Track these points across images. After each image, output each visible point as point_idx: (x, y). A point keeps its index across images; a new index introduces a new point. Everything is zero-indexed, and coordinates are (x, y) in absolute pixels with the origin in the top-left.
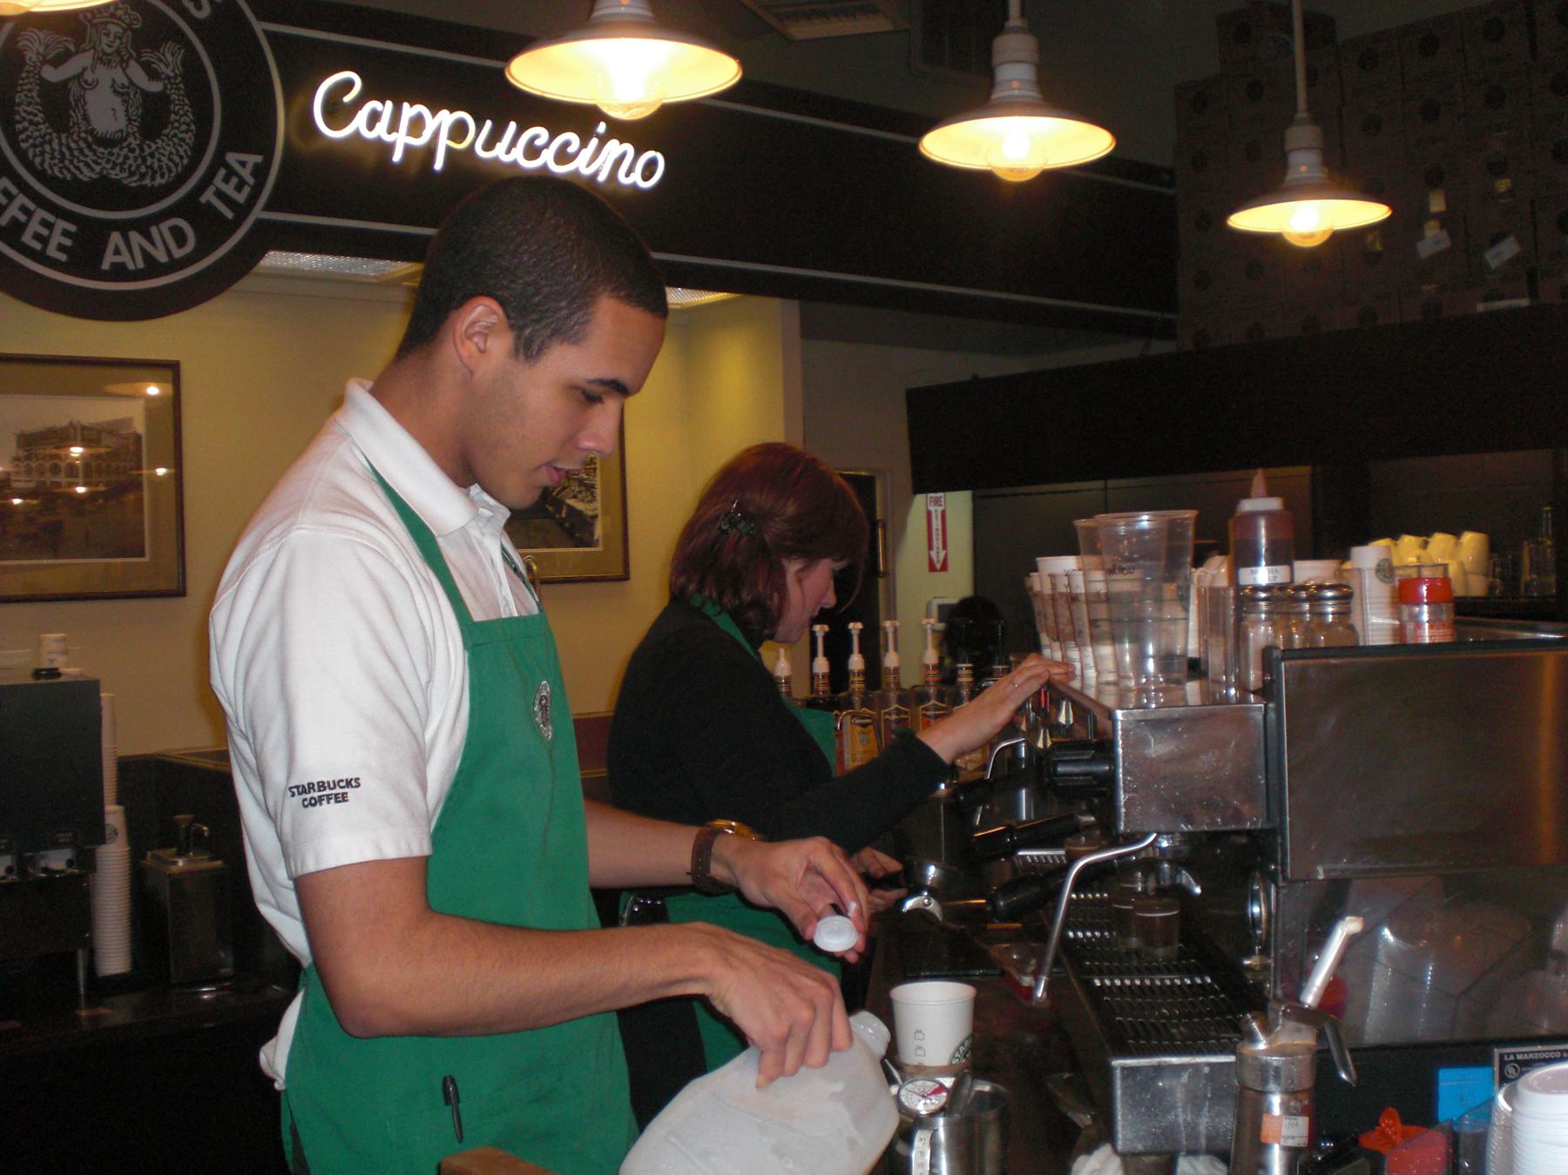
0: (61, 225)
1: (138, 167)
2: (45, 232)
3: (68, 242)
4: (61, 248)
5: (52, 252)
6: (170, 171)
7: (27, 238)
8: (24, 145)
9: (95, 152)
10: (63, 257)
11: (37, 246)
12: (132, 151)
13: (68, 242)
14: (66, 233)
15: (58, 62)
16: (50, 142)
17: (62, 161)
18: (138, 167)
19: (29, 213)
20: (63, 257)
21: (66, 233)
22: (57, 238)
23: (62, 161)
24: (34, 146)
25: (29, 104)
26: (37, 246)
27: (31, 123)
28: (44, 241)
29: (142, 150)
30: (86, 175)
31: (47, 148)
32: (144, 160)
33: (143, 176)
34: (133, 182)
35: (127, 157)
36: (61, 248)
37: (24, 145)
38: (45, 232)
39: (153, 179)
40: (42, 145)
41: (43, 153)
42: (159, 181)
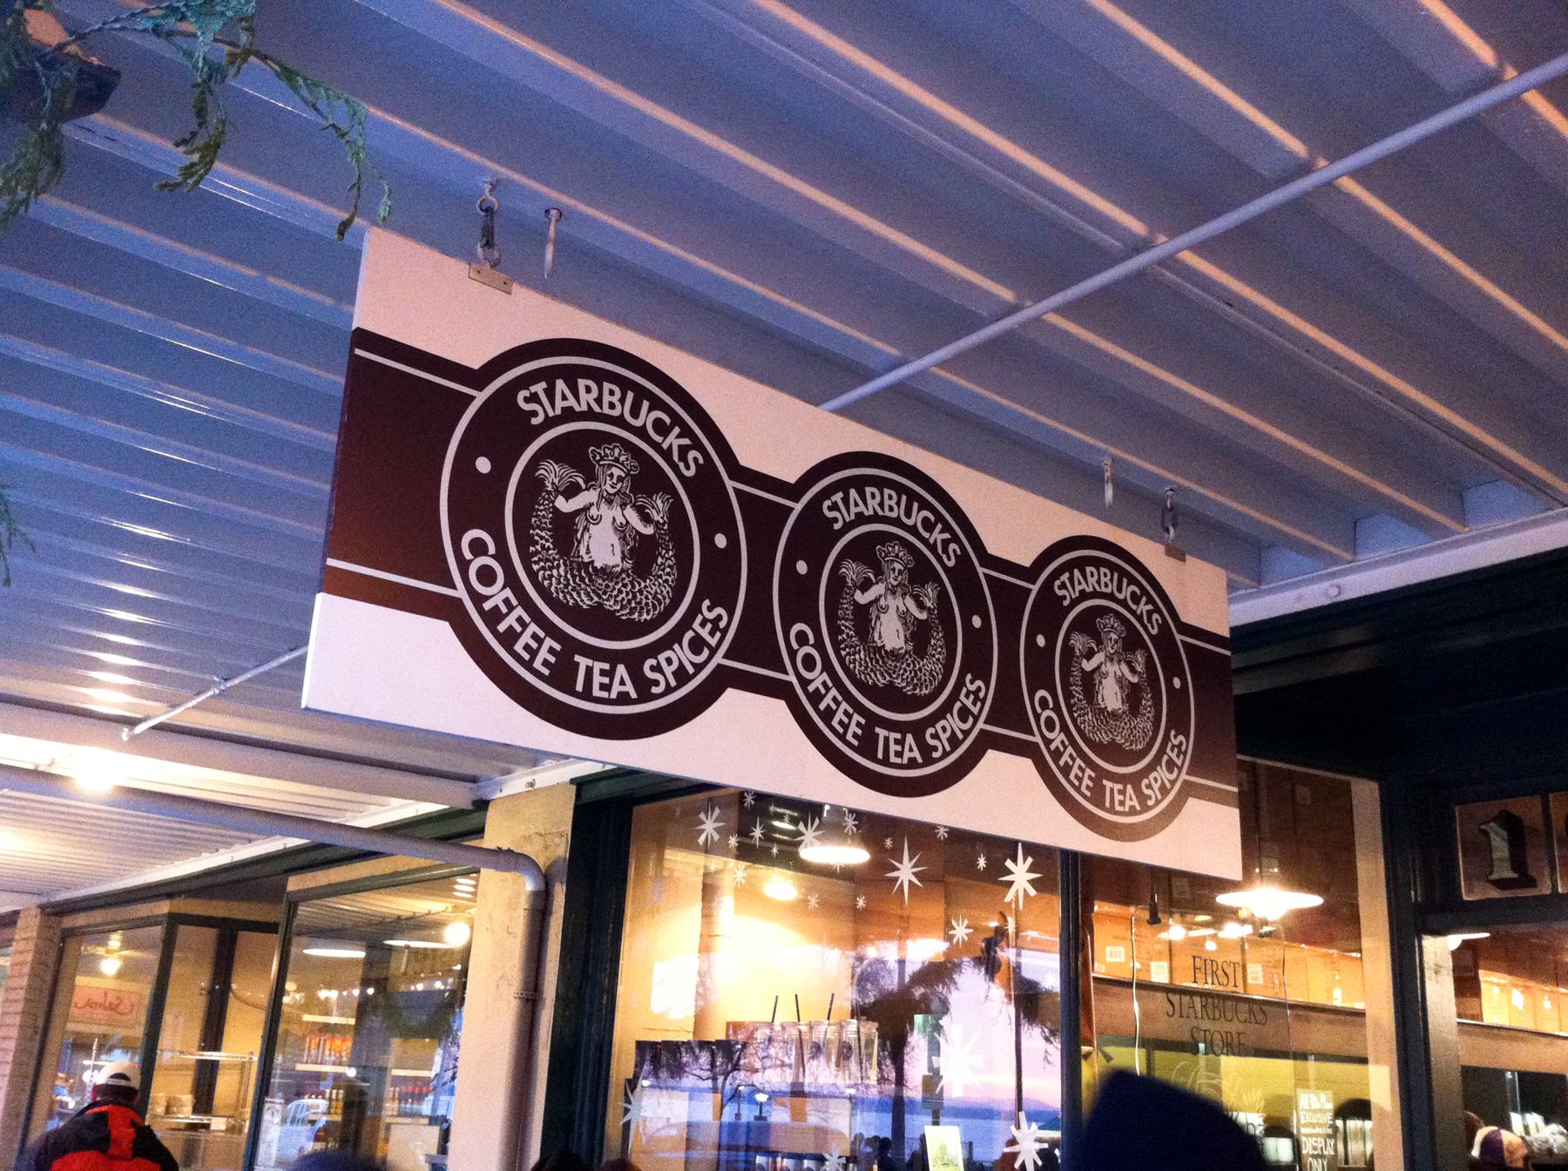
0: (549, 642)
1: (629, 602)
2: (534, 645)
3: (552, 659)
4: (546, 663)
5: (538, 664)
7: (518, 647)
8: (535, 567)
12: (625, 586)
13: (552, 659)
14: (551, 651)
16: (558, 566)
17: (566, 586)
18: (629, 602)
19: (524, 626)
20: (546, 672)
21: (551, 651)
22: (543, 654)
23: (566, 586)
24: (543, 568)
25: (542, 529)
27: (543, 547)
28: (534, 653)
30: (586, 603)
31: (555, 572)
32: (634, 597)
33: (631, 613)
34: (624, 614)
35: (620, 592)
36: (546, 663)
37: (535, 567)
38: (534, 645)
39: (640, 614)
40: (551, 568)
41: (551, 576)
42: (645, 616)
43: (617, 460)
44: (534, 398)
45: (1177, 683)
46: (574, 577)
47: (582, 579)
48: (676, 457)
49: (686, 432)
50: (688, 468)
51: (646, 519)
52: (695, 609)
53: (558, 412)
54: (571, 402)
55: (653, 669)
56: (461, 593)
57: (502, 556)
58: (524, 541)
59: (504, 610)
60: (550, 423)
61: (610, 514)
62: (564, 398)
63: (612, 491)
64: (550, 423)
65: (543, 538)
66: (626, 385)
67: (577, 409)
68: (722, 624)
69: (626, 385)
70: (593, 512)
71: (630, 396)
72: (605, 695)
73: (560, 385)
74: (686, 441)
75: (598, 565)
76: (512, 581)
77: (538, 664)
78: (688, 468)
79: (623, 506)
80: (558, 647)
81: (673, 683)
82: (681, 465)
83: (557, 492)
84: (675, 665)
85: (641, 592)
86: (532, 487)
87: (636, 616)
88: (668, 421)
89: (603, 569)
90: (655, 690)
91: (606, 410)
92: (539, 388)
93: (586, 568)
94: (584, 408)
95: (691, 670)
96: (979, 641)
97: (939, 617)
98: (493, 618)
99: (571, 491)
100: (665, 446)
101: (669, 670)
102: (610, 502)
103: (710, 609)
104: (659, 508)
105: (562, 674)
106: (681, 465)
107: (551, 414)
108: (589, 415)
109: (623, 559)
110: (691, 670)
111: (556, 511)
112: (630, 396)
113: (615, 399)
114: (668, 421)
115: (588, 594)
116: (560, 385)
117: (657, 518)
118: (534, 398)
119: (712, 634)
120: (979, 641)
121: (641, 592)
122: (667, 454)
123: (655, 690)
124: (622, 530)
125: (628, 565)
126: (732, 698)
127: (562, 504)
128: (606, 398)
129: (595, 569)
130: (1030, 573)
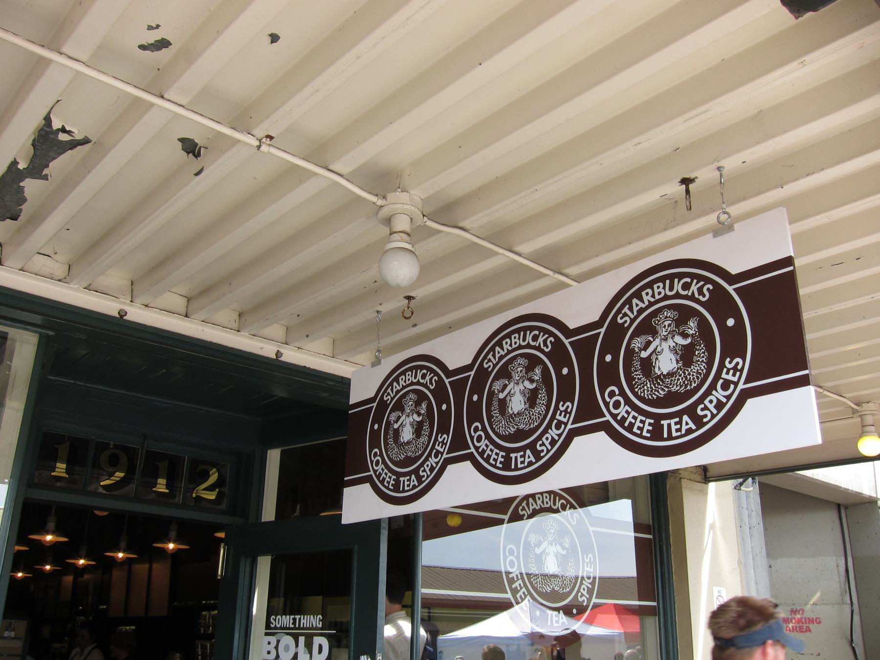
0: (648, 421)
3: (651, 428)
4: (648, 431)
5: (645, 434)
6: (698, 378)
9: (663, 382)
10: (649, 435)
11: (639, 432)
13: (651, 428)
14: (650, 424)
15: (645, 348)
20: (649, 435)
21: (650, 424)
22: (647, 427)
26: (639, 432)
29: (685, 373)
32: (686, 377)
33: (686, 387)
34: (682, 390)
35: (678, 380)
38: (641, 425)
42: (694, 385)
43: (666, 317)
44: (625, 315)
45: (376, 427)
46: (654, 385)
47: (659, 384)
48: (696, 295)
49: (700, 278)
50: (704, 296)
51: (685, 336)
52: (722, 365)
53: (635, 313)
54: (641, 305)
55: (702, 410)
56: (608, 417)
57: (622, 393)
58: (629, 379)
59: (626, 416)
60: (632, 321)
61: (665, 346)
62: (637, 305)
63: (665, 334)
64: (632, 321)
65: (638, 375)
66: (662, 279)
67: (643, 306)
68: (739, 367)
69: (662, 279)
70: (659, 349)
71: (668, 282)
72: (679, 434)
73: (635, 301)
74: (702, 283)
75: (665, 373)
76: (628, 402)
77: (645, 434)
78: (704, 296)
79: (673, 338)
80: (652, 421)
81: (715, 412)
82: (701, 298)
83: (641, 350)
84: (715, 401)
85: (689, 374)
86: (630, 352)
87: (689, 387)
88: (688, 280)
89: (668, 374)
90: (705, 420)
91: (657, 297)
92: (626, 310)
93: (662, 377)
94: (647, 303)
95: (724, 400)
96: (444, 417)
97: (701, 336)
98: (621, 422)
99: (648, 344)
100: (690, 294)
101: (711, 407)
102: (666, 339)
103: (730, 362)
104: (692, 326)
105: (656, 433)
106: (701, 298)
107: (632, 316)
108: (651, 304)
109: (677, 362)
110: (724, 400)
111: (641, 358)
112: (668, 282)
113: (661, 290)
114: (688, 280)
115: (662, 389)
116: (635, 301)
117: (691, 332)
118: (625, 315)
119: (734, 375)
120: (444, 417)
121: (689, 374)
122: (692, 298)
123: (705, 420)
124: (674, 350)
125: (680, 365)
126: (751, 403)
127: (644, 355)
128: (656, 291)
129: (664, 376)
130: (468, 368)
